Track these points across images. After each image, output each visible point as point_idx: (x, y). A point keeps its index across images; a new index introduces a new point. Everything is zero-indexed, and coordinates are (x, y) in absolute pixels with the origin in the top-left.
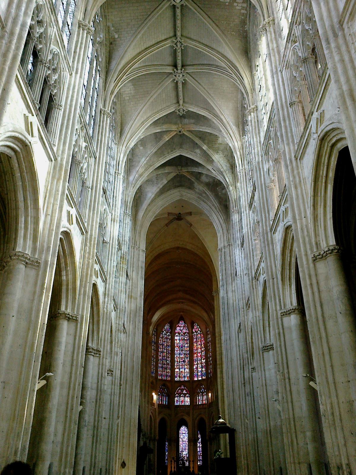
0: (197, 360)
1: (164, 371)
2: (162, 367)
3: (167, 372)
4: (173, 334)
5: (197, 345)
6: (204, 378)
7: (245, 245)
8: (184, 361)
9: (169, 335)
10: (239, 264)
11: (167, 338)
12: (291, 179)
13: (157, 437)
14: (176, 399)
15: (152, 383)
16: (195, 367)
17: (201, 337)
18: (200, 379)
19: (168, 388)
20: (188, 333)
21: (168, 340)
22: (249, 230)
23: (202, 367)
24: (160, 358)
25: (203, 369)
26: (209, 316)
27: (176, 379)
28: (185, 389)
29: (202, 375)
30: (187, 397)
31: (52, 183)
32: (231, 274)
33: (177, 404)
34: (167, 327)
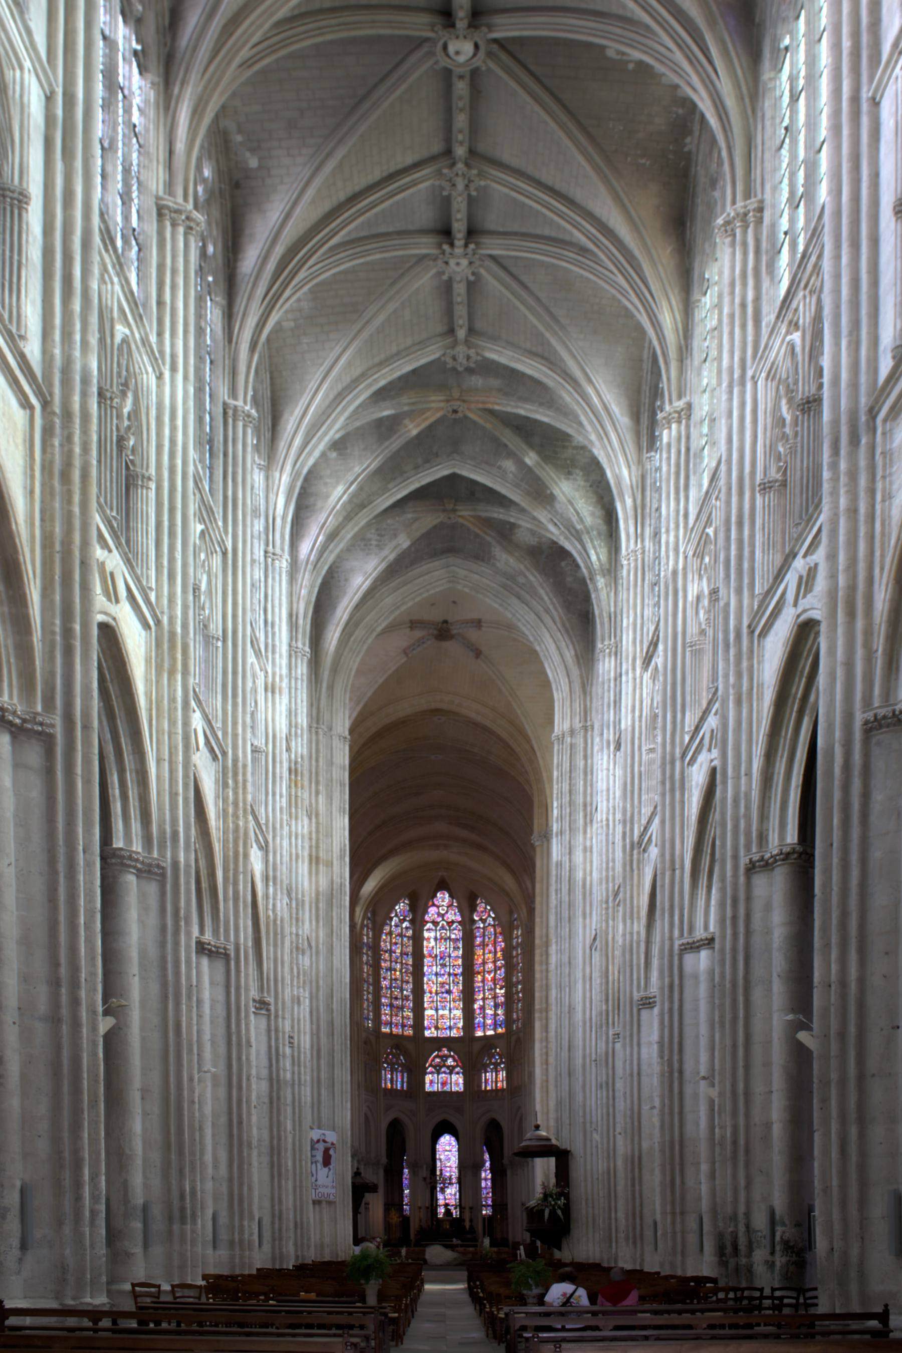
0: (484, 990)
3: (403, 1017)
4: (418, 924)
5: (484, 954)
6: (500, 1030)
7: (623, 748)
8: (449, 992)
9: (407, 928)
10: (605, 793)
11: (401, 935)
12: (732, 680)
14: (428, 1078)
16: (476, 1006)
17: (495, 934)
18: (490, 1033)
20: (459, 922)
22: (637, 723)
23: (496, 1006)
24: (385, 983)
26: (519, 882)
27: (427, 1033)
28: (450, 1056)
29: (495, 1025)
30: (458, 1073)
31: (157, 682)
32: (585, 805)
33: (431, 1089)
34: (401, 907)
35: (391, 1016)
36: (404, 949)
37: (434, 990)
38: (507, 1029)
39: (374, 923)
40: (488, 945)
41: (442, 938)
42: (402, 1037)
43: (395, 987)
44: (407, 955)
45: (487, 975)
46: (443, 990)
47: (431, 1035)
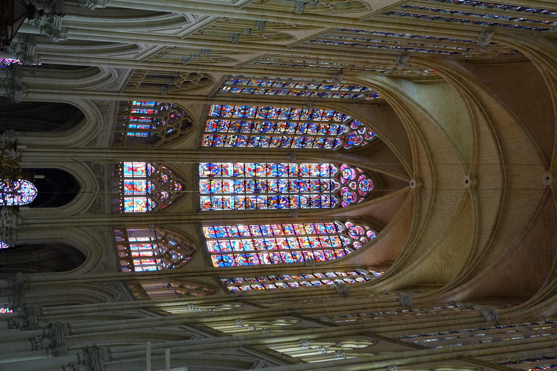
1: (230, 126)
2: (244, 119)
5: (306, 235)
6: (215, 260)
8: (257, 192)
13: (20, 97)
14: (140, 166)
15: (206, 79)
16: (241, 228)
17: (333, 249)
19: (177, 137)
21: (321, 141)
23: (246, 254)
25: (240, 259)
27: (203, 167)
29: (221, 253)
30: (147, 205)
35: (231, 119)
36: (310, 139)
37: (258, 174)
38: (219, 269)
39: (348, 102)
40: (319, 240)
41: (320, 183)
42: (203, 132)
43: (266, 125)
44: (303, 143)
45: (283, 239)
46: (260, 186)
47: (201, 170)
